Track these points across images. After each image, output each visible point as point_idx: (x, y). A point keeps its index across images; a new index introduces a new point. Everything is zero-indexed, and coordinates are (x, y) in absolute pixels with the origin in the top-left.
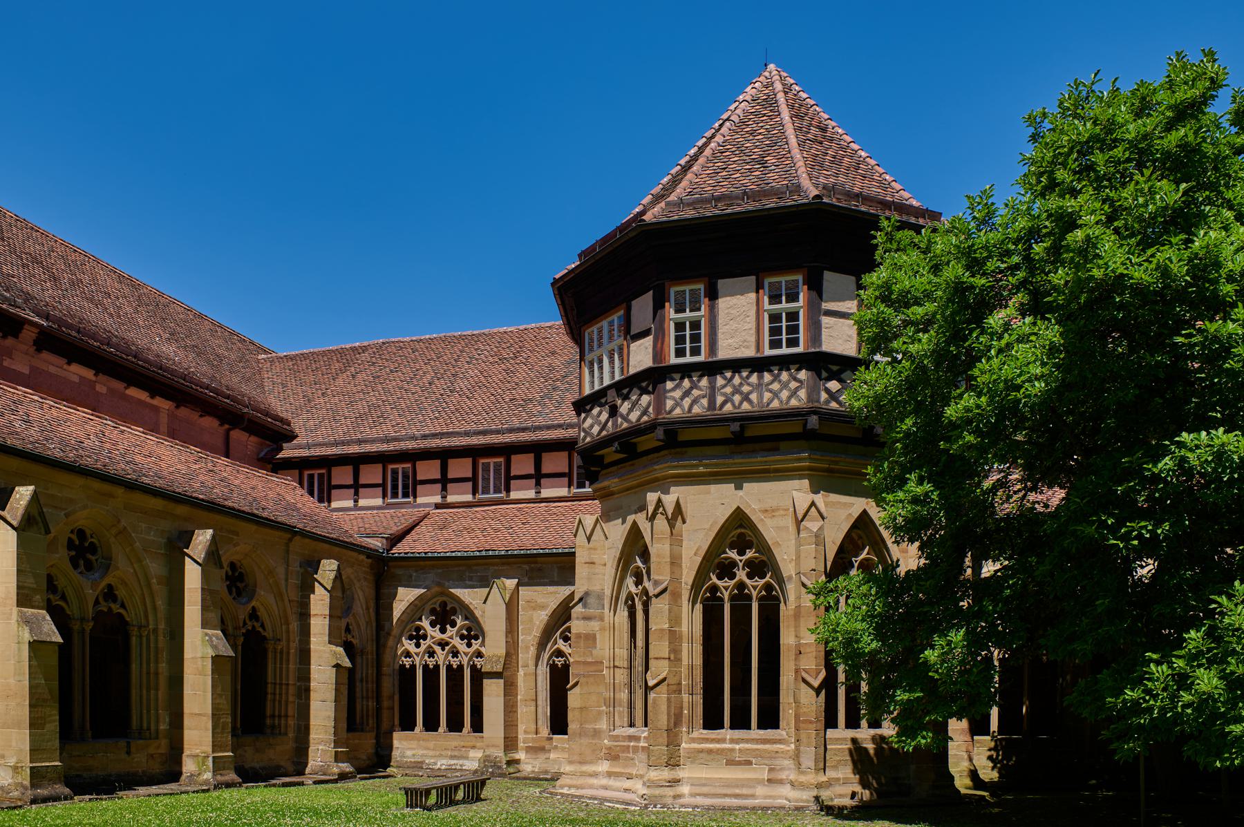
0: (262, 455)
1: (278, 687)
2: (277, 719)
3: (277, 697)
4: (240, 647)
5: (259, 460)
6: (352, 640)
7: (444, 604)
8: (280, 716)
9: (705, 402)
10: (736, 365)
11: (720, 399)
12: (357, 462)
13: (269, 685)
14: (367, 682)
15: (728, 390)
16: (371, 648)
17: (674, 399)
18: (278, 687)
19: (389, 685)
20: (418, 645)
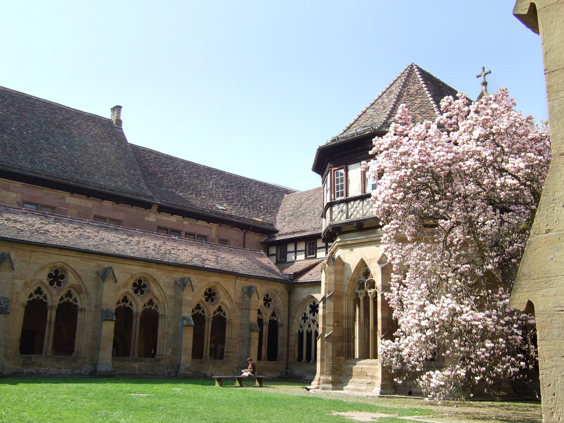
0: (262, 241)
1: (230, 339)
2: (229, 353)
3: (229, 344)
4: (210, 323)
5: (261, 243)
6: (277, 319)
7: (314, 303)
8: (230, 352)
9: (345, 215)
10: (355, 199)
11: (350, 214)
12: (295, 241)
13: (226, 339)
14: (283, 338)
15: (352, 210)
16: (286, 323)
17: (335, 215)
18: (230, 339)
19: (294, 340)
20: (305, 322)
